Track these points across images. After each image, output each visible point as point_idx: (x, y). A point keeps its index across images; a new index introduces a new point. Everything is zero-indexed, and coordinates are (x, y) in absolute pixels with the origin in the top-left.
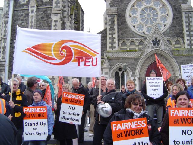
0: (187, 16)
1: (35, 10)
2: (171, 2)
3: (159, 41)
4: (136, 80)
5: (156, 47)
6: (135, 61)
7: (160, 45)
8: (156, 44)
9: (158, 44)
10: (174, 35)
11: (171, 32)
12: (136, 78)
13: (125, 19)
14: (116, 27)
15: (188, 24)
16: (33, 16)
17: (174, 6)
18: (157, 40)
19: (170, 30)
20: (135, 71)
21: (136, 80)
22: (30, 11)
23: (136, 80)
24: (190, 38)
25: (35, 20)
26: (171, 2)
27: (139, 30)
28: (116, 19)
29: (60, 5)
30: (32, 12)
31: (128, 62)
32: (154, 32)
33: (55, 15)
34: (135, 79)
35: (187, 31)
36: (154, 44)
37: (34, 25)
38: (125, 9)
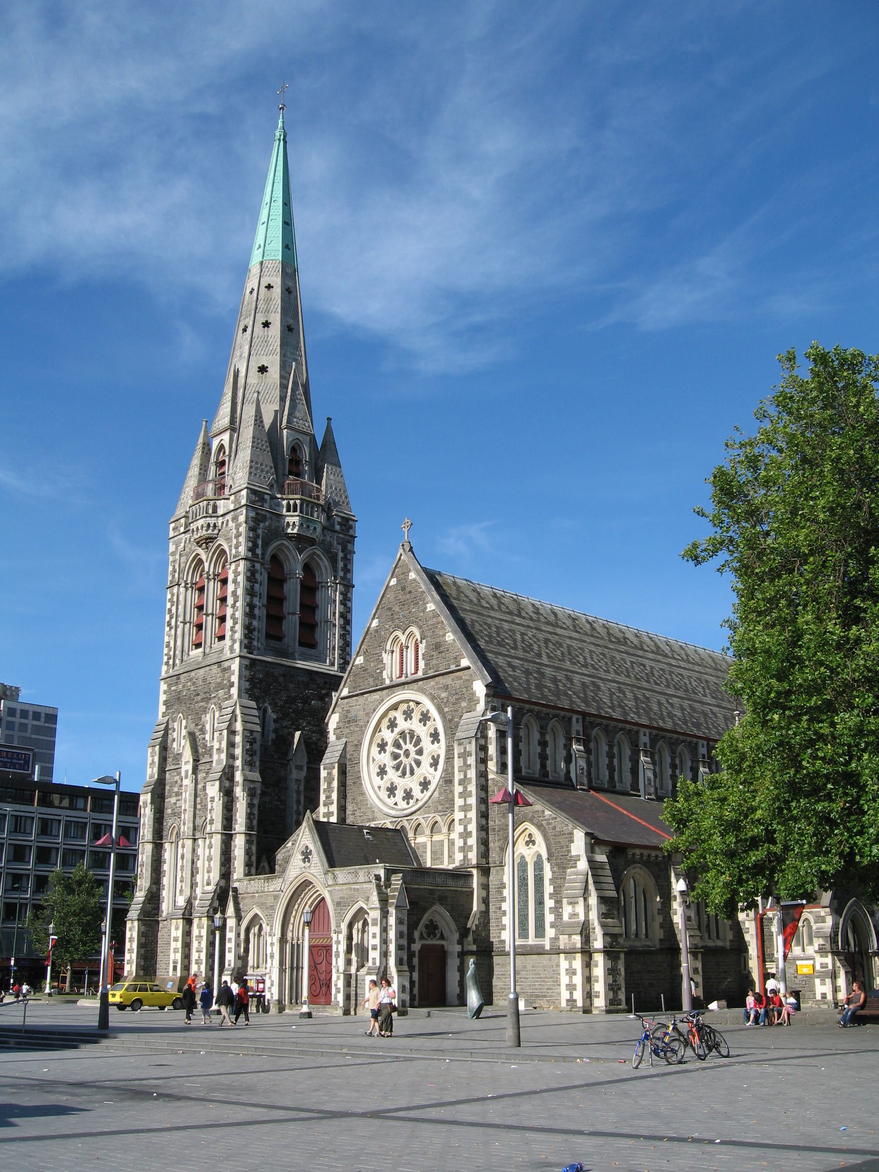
0: (462, 751)
1: (190, 772)
2: (446, 710)
10: (447, 806)
11: (441, 798)
13: (359, 772)
14: (334, 796)
15: (462, 777)
16: (186, 786)
17: (450, 721)
19: (440, 794)
22: (183, 774)
24: (465, 816)
25: (190, 795)
26: (446, 710)
27: (389, 797)
28: (335, 772)
29: (224, 756)
30: (186, 777)
33: (212, 785)
35: (461, 795)
37: (190, 807)
38: (358, 746)
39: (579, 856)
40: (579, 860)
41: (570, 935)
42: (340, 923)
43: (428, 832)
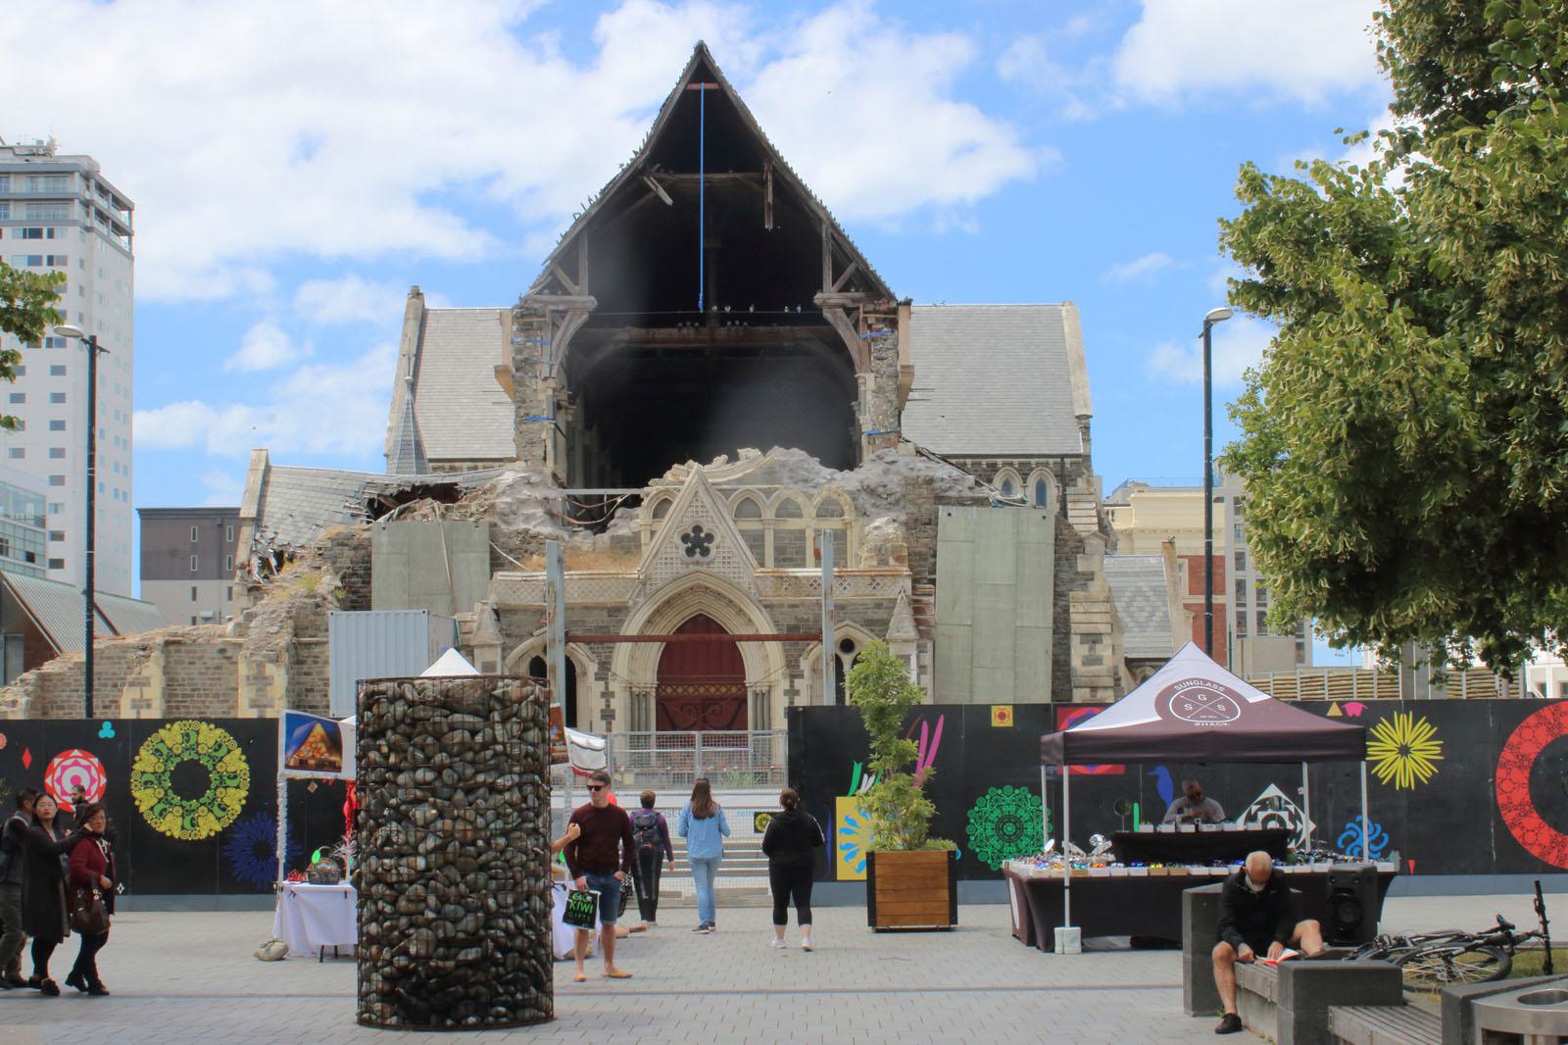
3: (710, 538)
4: (613, 693)
5: (698, 563)
6: (610, 616)
7: (713, 552)
8: (698, 550)
9: (705, 552)
12: (614, 686)
18: (702, 535)
20: (610, 657)
21: (612, 694)
23: (613, 693)
31: (583, 622)
32: (692, 502)
34: (610, 690)
36: (690, 552)
39: (1093, 573)
40: (1093, 579)
41: (1094, 689)
42: (797, 661)
43: (769, 514)
